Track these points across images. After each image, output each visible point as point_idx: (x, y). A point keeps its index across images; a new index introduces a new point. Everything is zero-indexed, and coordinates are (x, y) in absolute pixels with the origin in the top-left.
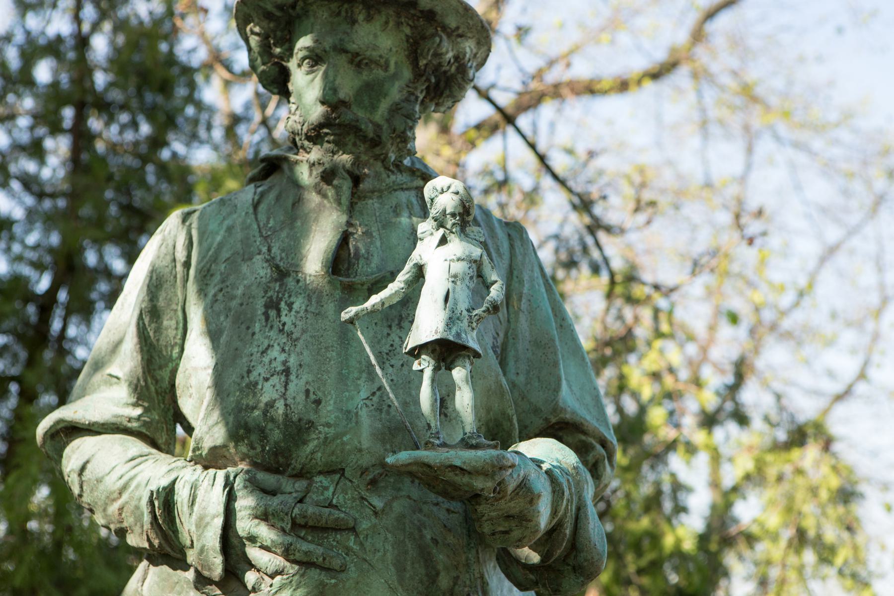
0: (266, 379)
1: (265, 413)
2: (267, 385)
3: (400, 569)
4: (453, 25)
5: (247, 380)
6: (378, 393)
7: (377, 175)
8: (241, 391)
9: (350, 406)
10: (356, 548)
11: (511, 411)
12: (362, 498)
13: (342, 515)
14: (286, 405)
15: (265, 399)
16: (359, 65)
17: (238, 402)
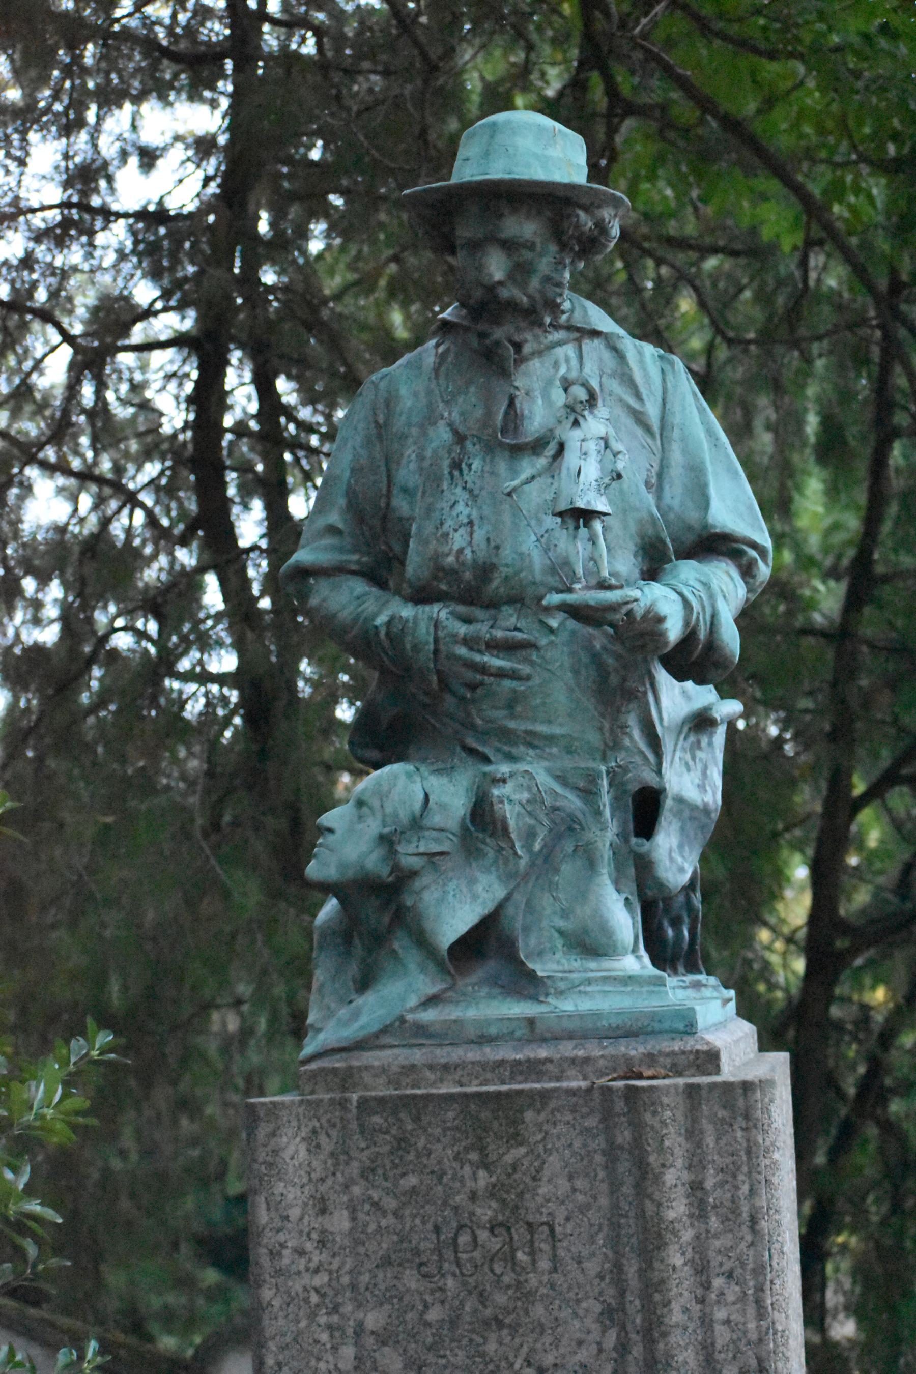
0: (456, 530)
1: (457, 558)
2: (457, 536)
3: (576, 672)
4: (588, 202)
5: (440, 533)
6: (546, 535)
7: (536, 337)
8: (438, 540)
9: (524, 548)
10: (539, 661)
11: (665, 535)
12: (541, 621)
13: (525, 636)
14: (473, 552)
15: (456, 547)
16: (509, 249)
17: (436, 550)
